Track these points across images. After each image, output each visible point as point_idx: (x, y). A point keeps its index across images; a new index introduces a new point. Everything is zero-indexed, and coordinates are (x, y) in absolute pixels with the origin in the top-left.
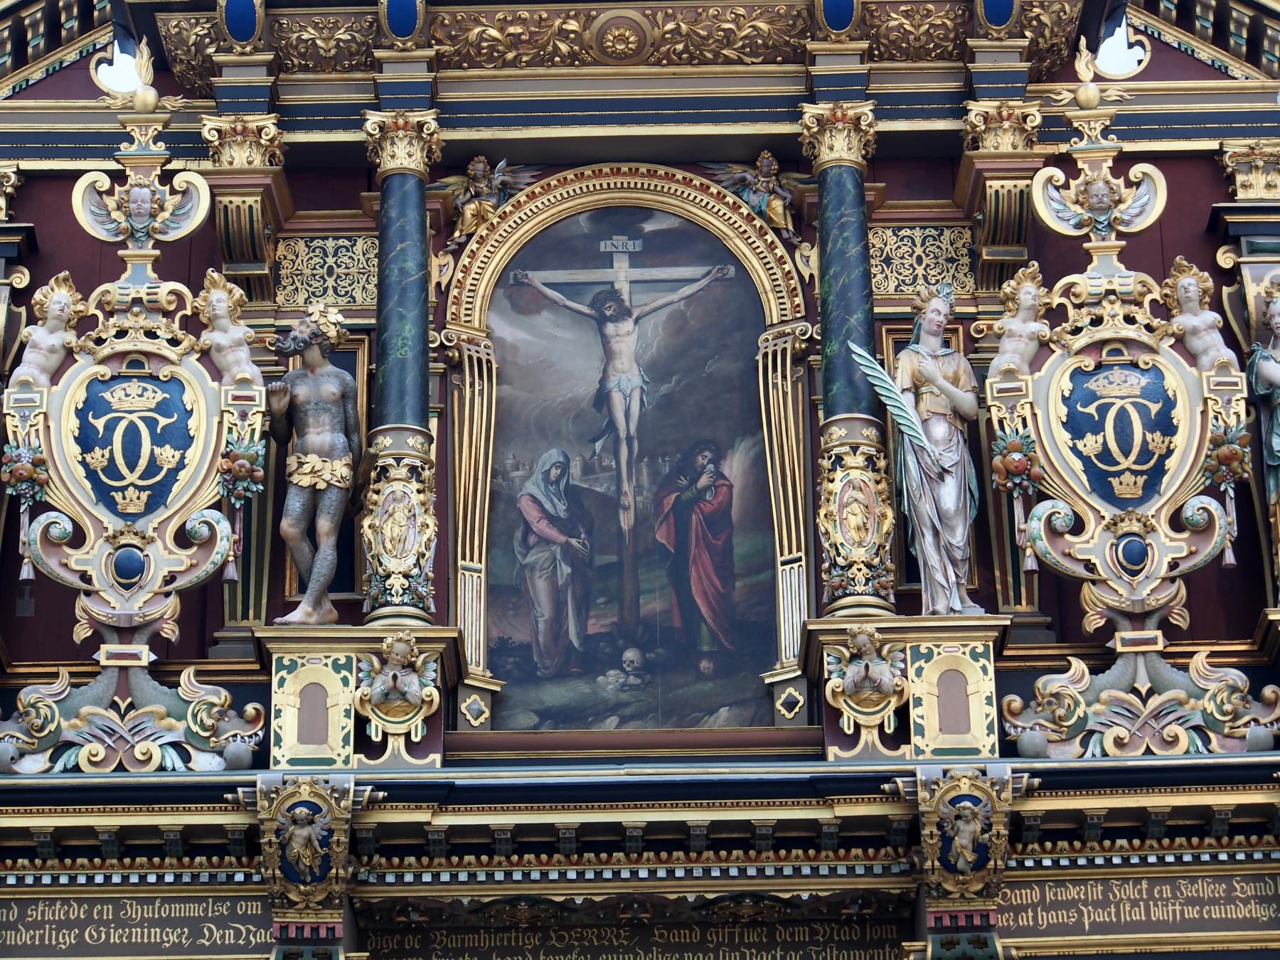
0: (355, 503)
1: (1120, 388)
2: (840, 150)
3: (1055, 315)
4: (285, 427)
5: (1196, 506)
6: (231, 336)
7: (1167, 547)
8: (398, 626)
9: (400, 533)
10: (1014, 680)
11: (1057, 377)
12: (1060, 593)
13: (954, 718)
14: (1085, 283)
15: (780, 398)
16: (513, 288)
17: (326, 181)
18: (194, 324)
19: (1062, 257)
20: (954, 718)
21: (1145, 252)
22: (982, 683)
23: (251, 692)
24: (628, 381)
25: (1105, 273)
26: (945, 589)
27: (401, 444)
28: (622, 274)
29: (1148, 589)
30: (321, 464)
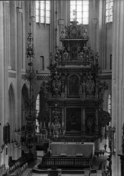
0: (64, 88)
1: (90, 85)
2: (81, 75)
3: (88, 82)
4: (62, 85)
5: (93, 89)
6: (60, 82)
7: (92, 91)
8: (66, 93)
9: (66, 89)
10: (86, 95)
11: (88, 85)
12: (88, 92)
13: (84, 97)
14: (89, 80)
15: (79, 82)
16: (70, 78)
17: (63, 75)
18: (59, 82)
19: (89, 79)
20: (84, 97)
21: (91, 79)
22: (85, 95)
23: (61, 95)
24: (74, 81)
25: (90, 80)
26: (84, 92)
27: (66, 86)
28: (74, 77)
29: (91, 92)
30: (63, 87)
